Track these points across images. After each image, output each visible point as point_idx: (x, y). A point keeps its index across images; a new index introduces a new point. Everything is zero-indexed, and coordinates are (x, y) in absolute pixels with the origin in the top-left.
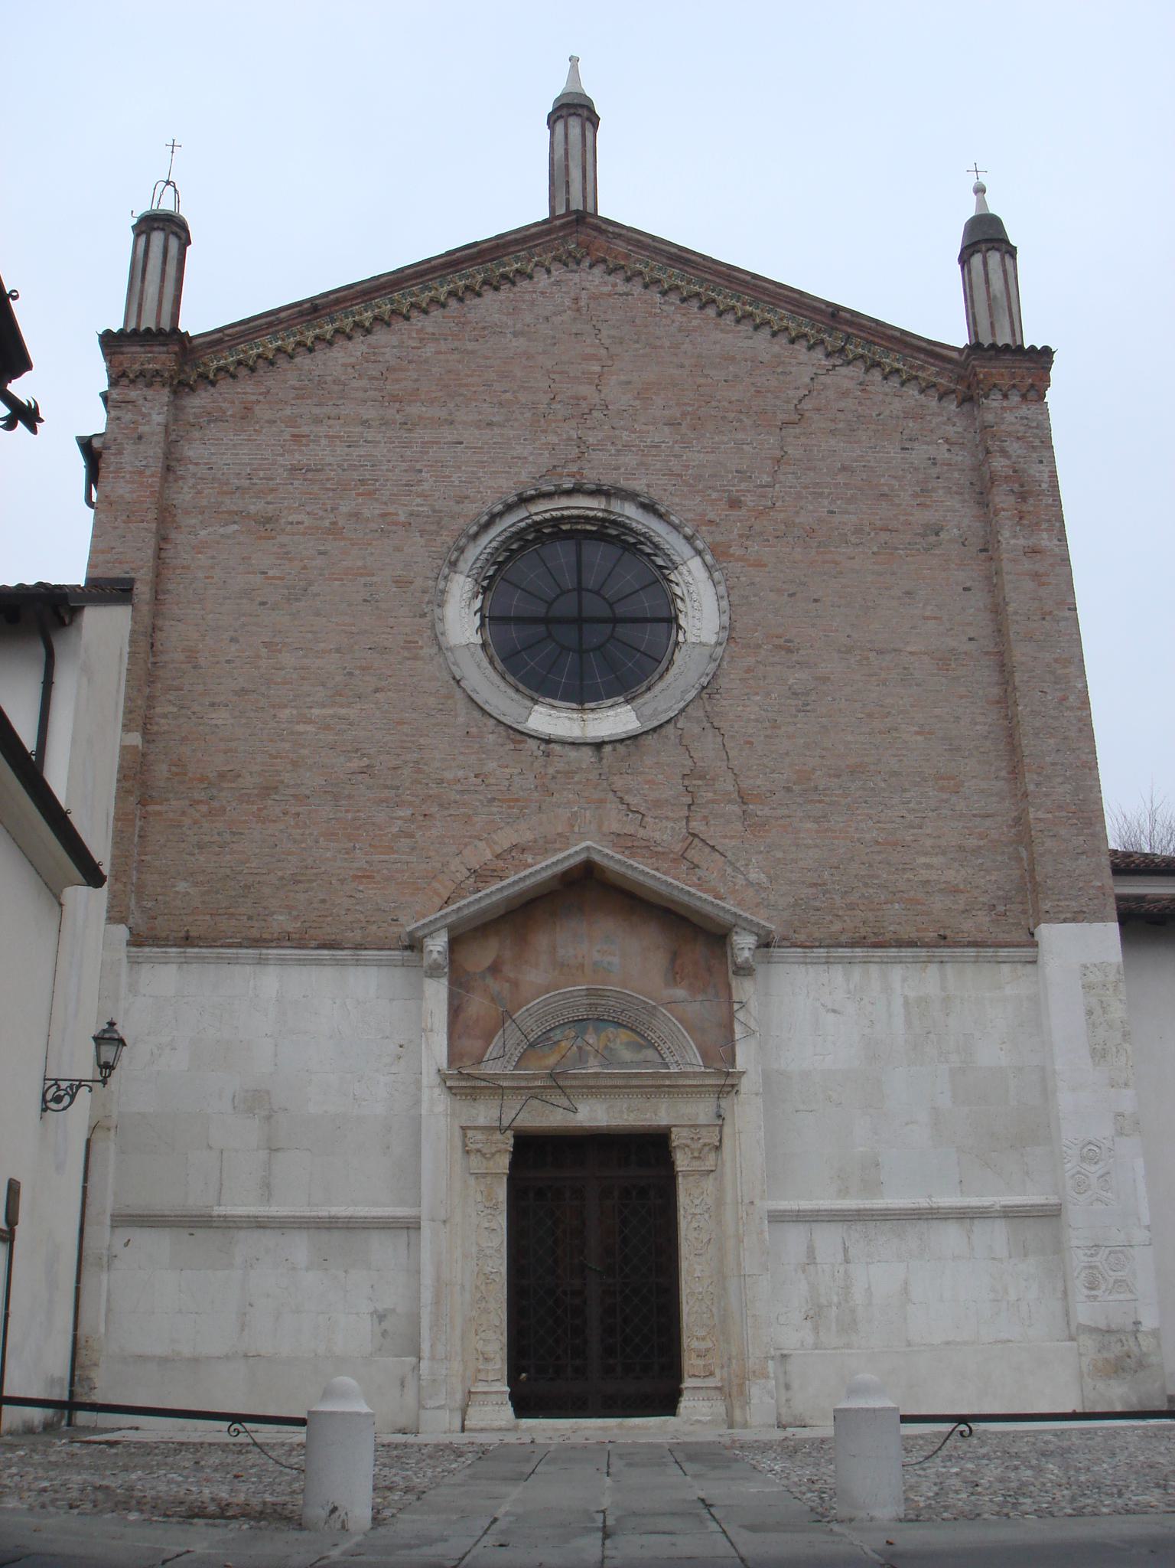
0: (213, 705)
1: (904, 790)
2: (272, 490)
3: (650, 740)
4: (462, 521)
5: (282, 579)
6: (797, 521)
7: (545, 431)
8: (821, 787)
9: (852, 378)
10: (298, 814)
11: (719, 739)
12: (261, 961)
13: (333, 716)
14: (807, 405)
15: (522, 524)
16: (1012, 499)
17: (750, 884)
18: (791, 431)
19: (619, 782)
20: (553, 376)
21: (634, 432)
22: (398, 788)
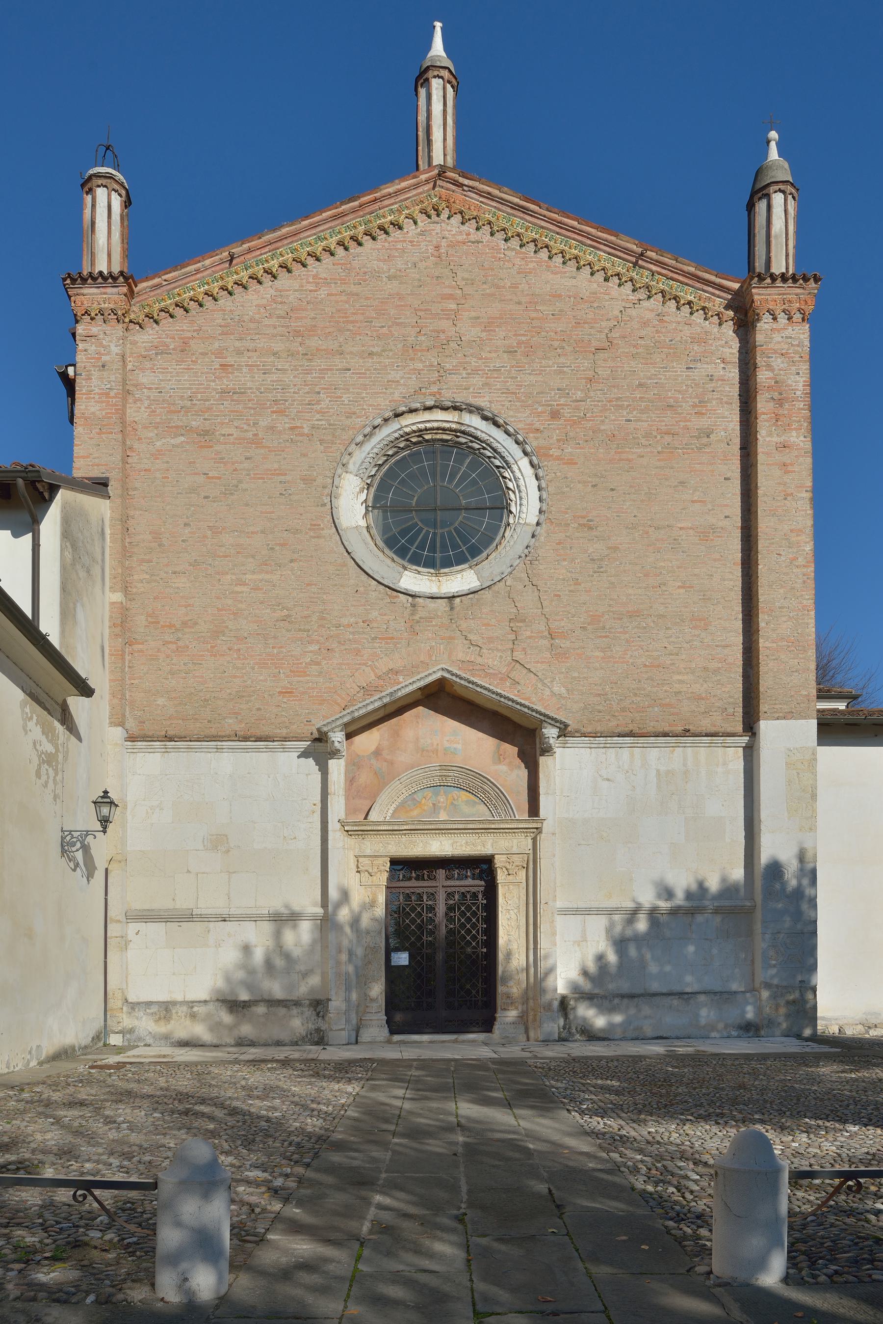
0: (175, 573)
1: (667, 628)
2: (209, 409)
3: (487, 595)
4: (351, 432)
5: (219, 478)
6: (602, 428)
7: (412, 359)
8: (607, 627)
9: (652, 310)
10: (239, 650)
11: (536, 593)
12: (218, 749)
13: (261, 580)
14: (615, 334)
15: (396, 435)
16: (771, 404)
17: (553, 694)
18: (601, 355)
19: (464, 625)
20: (419, 313)
21: (481, 359)
22: (309, 631)
